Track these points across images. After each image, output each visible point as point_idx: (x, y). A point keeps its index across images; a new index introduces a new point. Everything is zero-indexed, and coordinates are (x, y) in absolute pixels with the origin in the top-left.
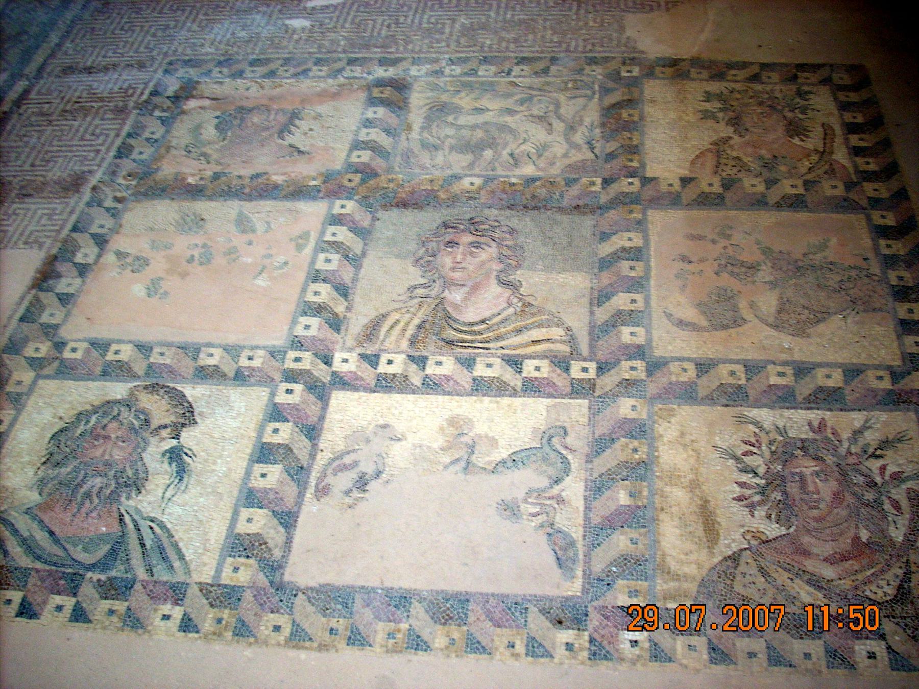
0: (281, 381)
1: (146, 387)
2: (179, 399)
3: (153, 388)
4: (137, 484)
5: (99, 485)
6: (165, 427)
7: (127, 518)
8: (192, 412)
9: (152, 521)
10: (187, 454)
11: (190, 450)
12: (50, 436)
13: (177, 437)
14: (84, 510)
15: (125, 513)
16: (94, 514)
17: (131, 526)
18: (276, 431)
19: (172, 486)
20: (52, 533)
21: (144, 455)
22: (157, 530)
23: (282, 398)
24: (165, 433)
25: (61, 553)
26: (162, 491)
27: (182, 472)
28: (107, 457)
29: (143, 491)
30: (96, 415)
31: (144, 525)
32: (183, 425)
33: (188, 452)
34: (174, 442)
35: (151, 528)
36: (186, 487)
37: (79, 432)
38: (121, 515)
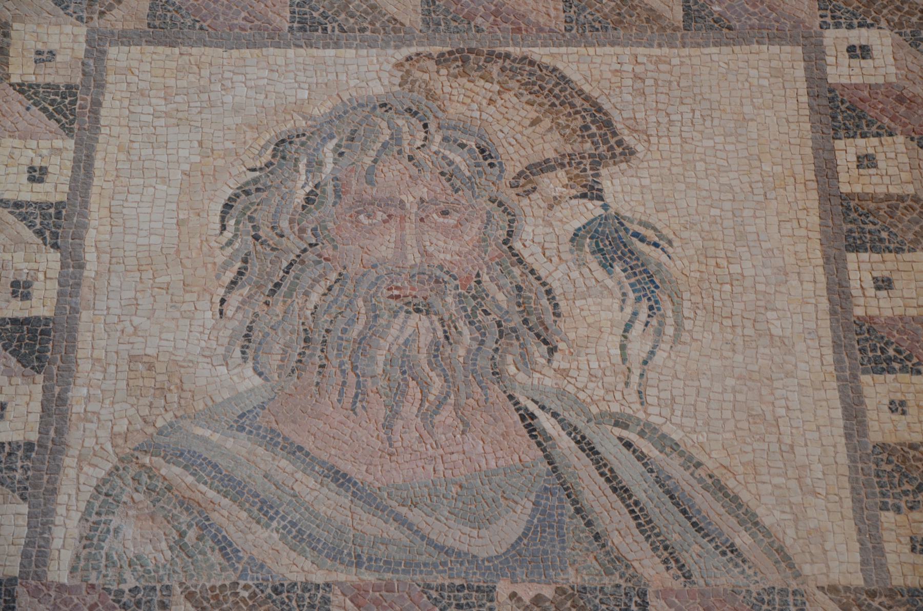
0: (824, 26)
1: (441, 60)
2: (552, 92)
3: (460, 60)
4: (536, 324)
5: (425, 339)
6: (545, 167)
7: (546, 422)
8: (608, 124)
9: (626, 427)
10: (642, 240)
11: (646, 225)
12: (220, 208)
13: (593, 192)
14: (410, 410)
15: (532, 407)
16: (447, 415)
17: (565, 443)
18: (866, 161)
19: (638, 327)
20: (341, 479)
21: (518, 245)
22: (644, 445)
23: (841, 72)
24: (554, 183)
25: (392, 530)
26: (617, 340)
27: (647, 283)
28: (413, 257)
29: (561, 345)
30: (331, 145)
31: (607, 441)
32: (597, 161)
33: (642, 231)
34: (593, 209)
35: (628, 445)
36: (678, 326)
37: (300, 197)
38: (527, 417)
